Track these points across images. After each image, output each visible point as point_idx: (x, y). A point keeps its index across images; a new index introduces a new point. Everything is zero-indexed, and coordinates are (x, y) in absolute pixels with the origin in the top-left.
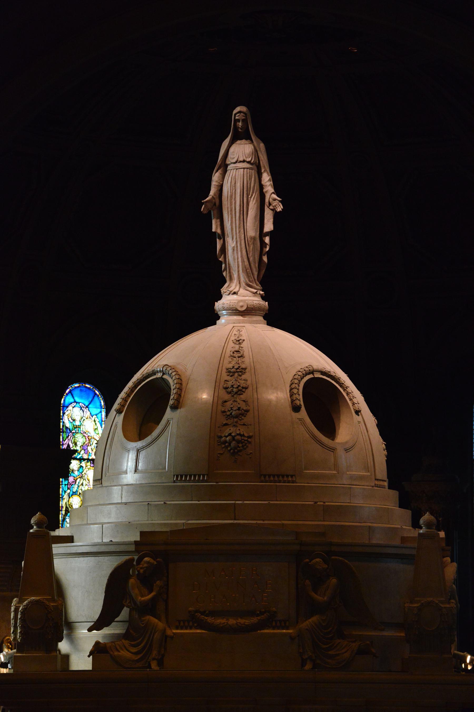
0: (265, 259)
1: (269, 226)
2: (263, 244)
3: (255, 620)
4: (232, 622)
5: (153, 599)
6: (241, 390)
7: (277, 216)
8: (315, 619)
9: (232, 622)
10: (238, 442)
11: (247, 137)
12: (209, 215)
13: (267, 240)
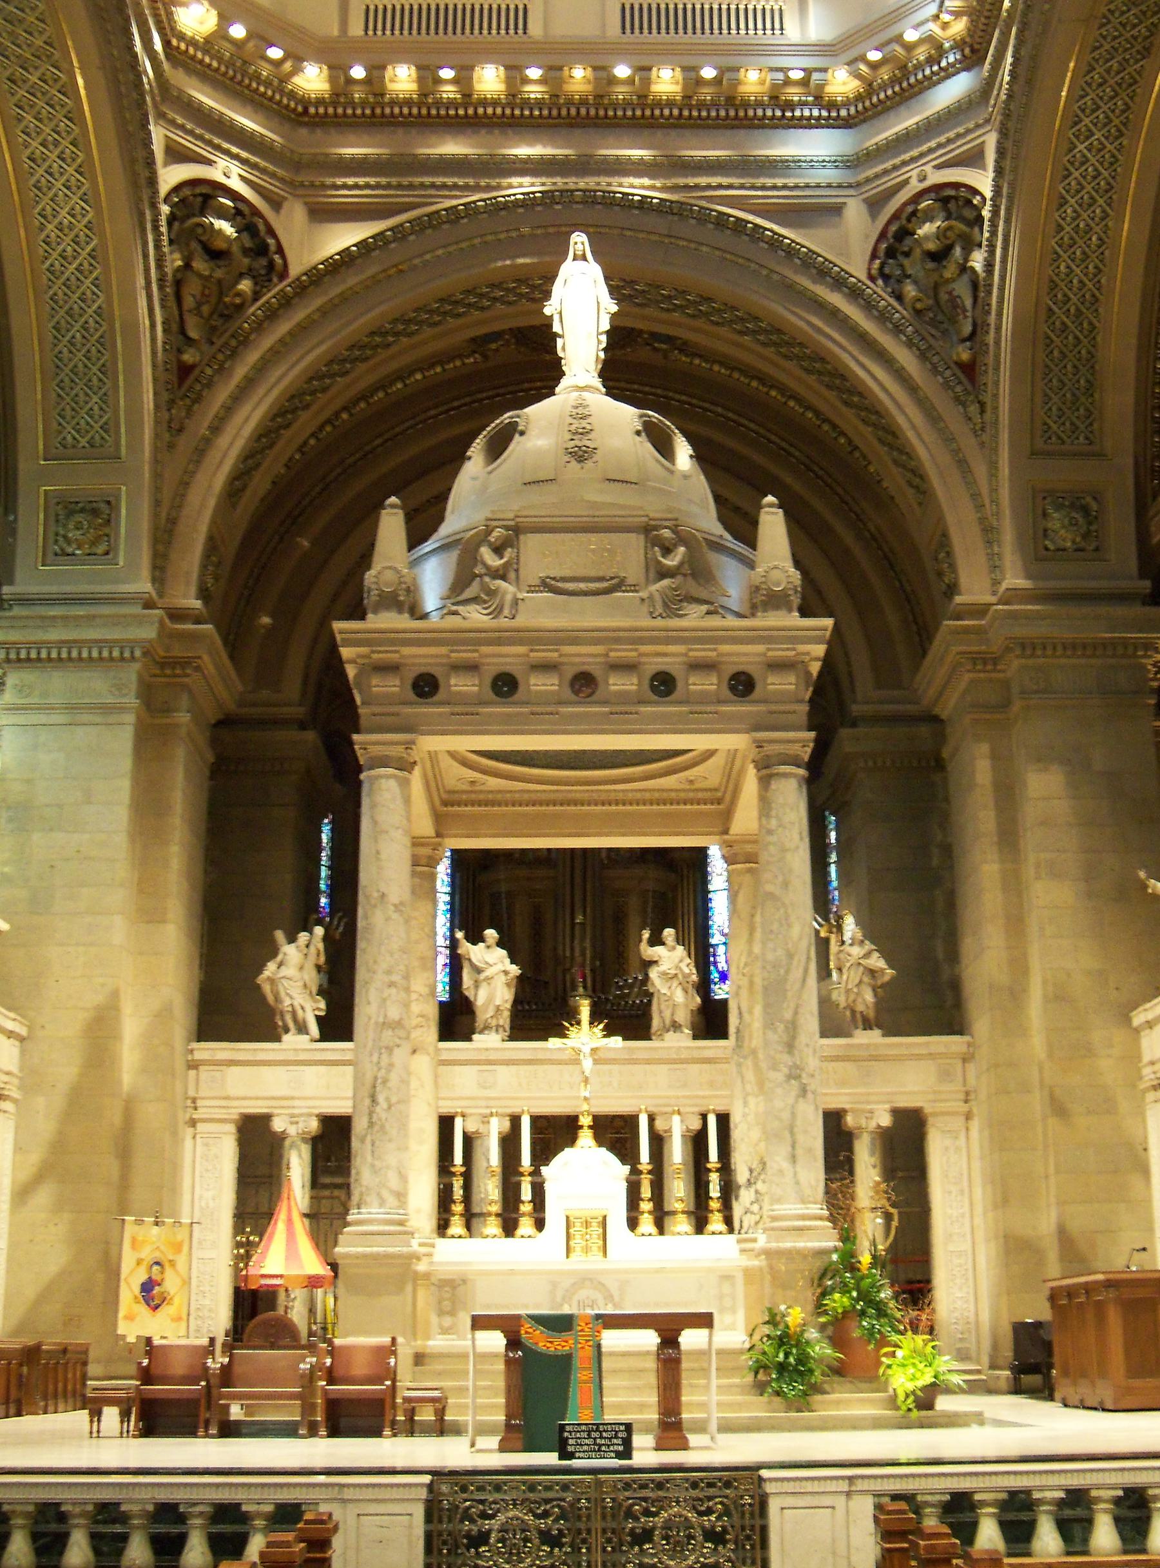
3: (605, 584)
4: (582, 586)
5: (506, 565)
8: (666, 582)
9: (582, 586)
10: (585, 452)
11: (584, 258)
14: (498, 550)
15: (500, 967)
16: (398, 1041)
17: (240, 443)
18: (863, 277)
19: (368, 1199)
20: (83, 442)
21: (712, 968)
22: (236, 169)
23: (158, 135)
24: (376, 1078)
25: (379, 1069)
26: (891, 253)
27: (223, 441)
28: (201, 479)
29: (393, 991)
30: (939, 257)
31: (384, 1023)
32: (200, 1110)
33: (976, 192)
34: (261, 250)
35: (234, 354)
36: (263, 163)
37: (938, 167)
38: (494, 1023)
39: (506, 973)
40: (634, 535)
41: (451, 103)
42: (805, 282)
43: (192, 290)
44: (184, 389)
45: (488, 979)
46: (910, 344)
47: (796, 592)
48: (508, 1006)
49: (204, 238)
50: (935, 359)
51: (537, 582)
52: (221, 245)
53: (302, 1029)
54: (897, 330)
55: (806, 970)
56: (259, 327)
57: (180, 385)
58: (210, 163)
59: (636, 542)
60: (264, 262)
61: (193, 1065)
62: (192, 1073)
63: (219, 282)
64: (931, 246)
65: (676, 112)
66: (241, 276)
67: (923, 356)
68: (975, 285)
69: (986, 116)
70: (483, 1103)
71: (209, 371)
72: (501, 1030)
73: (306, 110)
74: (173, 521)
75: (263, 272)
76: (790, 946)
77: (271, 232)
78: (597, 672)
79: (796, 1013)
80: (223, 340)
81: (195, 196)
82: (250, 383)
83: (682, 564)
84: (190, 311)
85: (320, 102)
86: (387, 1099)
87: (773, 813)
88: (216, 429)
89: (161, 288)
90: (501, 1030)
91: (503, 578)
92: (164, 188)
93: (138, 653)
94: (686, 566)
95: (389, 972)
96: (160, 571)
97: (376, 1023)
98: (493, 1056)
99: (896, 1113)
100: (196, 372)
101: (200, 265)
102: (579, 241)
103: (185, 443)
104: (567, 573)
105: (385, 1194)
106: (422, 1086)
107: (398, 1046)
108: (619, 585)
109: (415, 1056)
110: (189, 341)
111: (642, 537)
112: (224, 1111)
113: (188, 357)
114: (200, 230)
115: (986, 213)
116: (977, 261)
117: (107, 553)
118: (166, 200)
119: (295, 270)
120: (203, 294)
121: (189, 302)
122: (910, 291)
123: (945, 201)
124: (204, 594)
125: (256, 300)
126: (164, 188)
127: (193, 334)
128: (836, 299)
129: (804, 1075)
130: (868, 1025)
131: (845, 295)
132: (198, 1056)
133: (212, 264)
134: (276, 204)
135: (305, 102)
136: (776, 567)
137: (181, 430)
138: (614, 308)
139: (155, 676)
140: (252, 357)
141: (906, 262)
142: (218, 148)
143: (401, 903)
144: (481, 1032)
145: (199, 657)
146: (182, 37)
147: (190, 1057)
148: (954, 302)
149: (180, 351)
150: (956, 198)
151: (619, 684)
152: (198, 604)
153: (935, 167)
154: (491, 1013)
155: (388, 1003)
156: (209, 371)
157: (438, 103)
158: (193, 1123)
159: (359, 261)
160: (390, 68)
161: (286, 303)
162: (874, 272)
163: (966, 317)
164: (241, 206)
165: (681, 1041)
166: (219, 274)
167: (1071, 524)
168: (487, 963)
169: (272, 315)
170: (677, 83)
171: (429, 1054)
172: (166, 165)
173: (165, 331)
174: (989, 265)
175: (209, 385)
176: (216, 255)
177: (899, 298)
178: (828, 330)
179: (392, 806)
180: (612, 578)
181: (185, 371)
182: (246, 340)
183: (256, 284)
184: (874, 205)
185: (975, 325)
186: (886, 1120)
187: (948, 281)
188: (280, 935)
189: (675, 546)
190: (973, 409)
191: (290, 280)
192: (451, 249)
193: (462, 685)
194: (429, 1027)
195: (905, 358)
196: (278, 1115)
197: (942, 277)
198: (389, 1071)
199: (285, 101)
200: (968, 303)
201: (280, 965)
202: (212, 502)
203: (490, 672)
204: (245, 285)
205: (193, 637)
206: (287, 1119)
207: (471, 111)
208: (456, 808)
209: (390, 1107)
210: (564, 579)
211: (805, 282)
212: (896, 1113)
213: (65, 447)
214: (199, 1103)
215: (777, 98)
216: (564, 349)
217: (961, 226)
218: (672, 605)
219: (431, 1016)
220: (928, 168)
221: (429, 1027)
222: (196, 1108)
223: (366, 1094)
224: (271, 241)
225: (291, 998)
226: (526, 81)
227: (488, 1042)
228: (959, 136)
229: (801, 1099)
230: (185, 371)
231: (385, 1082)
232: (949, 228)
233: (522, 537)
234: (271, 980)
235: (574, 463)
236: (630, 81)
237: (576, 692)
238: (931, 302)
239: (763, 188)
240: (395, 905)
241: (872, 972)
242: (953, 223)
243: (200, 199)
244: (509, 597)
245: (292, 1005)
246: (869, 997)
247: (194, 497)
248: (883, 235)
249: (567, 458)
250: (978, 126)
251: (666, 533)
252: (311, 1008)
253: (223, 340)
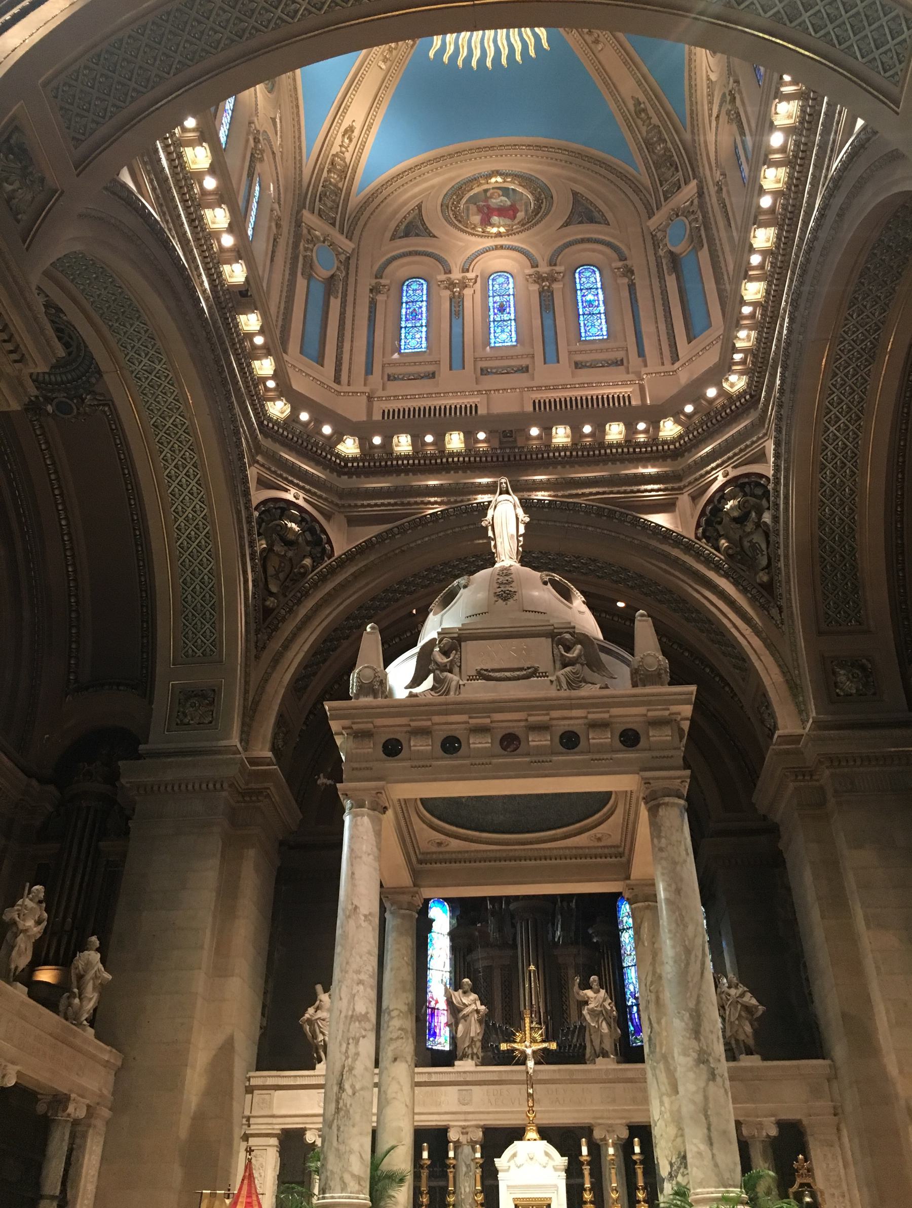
0: (520, 549)
1: (522, 530)
2: (518, 541)
4: (508, 674)
5: (451, 661)
6: (509, 583)
7: (527, 526)
8: (568, 669)
9: (508, 674)
11: (508, 493)
12: (486, 528)
13: (521, 539)
14: (445, 653)
15: (473, 1007)
16: (364, 1033)
17: (301, 655)
18: (693, 537)
19: (332, 1184)
20: (199, 653)
21: (630, 1023)
22: (301, 495)
23: (252, 473)
24: (344, 1067)
25: (347, 1058)
26: (708, 523)
27: (290, 654)
28: (276, 676)
29: (361, 987)
30: (740, 520)
31: (352, 1016)
32: (252, 1127)
33: (762, 476)
34: (318, 542)
35: (299, 602)
36: (319, 493)
37: (735, 467)
38: (470, 1051)
39: (477, 1011)
40: (543, 639)
41: (433, 457)
42: (654, 543)
43: (273, 562)
44: (266, 624)
45: (465, 1017)
46: (726, 576)
47: (666, 671)
48: (480, 1037)
49: (281, 533)
50: (745, 583)
51: (474, 673)
52: (291, 537)
54: (717, 568)
55: (703, 963)
56: (315, 586)
57: (264, 620)
58: (286, 490)
59: (546, 643)
60: (319, 549)
61: (250, 1090)
62: (249, 1096)
63: (291, 559)
64: (736, 514)
65: (568, 453)
66: (305, 557)
67: (736, 583)
68: (767, 535)
69: (764, 431)
70: (462, 1117)
71: (283, 612)
72: (475, 1057)
73: (346, 465)
74: (256, 703)
75: (319, 555)
76: (687, 943)
77: (324, 531)
78: (520, 732)
79: (698, 1002)
80: (292, 594)
81: (276, 509)
82: (308, 619)
83: (579, 656)
84: (272, 576)
85: (354, 459)
86: (353, 1087)
87: (663, 834)
88: (286, 646)
89: (252, 559)
90: (475, 1057)
91: (451, 671)
92: (255, 502)
93: (225, 785)
94: (583, 658)
95: (358, 972)
97: (346, 1017)
98: (469, 1078)
99: (781, 1124)
100: (275, 612)
101: (279, 548)
103: (267, 656)
104: (496, 666)
105: (347, 1177)
106: (402, 1090)
107: (364, 1037)
108: (534, 672)
109: (396, 1063)
110: (271, 594)
111: (550, 640)
112: (270, 1127)
113: (271, 602)
114: (279, 528)
115: (770, 487)
116: (767, 518)
117: (211, 722)
118: (256, 509)
120: (280, 566)
121: (271, 571)
122: (724, 543)
123: (742, 487)
124: (274, 749)
125: (313, 571)
126: (255, 502)
127: (274, 589)
128: (676, 552)
129: (711, 1060)
130: (750, 1052)
131: (682, 550)
132: (253, 1082)
133: (286, 548)
134: (328, 517)
135: (346, 460)
136: (649, 655)
137: (264, 648)
138: (527, 519)
139: (238, 802)
140: (310, 603)
141: (719, 527)
142: (292, 482)
143: (370, 914)
144: (461, 1059)
145: (268, 788)
146: (270, 419)
147: (247, 1084)
148: (753, 546)
149: (264, 600)
150: (749, 484)
151: (537, 740)
152: (270, 754)
153: (733, 467)
154: (467, 1044)
155: (356, 998)
156: (283, 612)
157: (425, 457)
158: (246, 1137)
159: (377, 546)
160: (395, 437)
161: (332, 571)
162: (699, 535)
163: (763, 555)
164: (304, 515)
165: (607, 1065)
166: (290, 554)
167: (854, 677)
168: (464, 1004)
169: (323, 579)
170: (568, 437)
171: (407, 1062)
172: (257, 489)
173: (254, 586)
174: (776, 519)
175: (284, 620)
176: (289, 543)
177: (718, 549)
178: (672, 571)
179: (365, 837)
180: (529, 668)
181: (267, 612)
182: (306, 594)
183: (314, 562)
184: (695, 498)
185: (769, 559)
186: (774, 1132)
187: (749, 534)
188: (319, 988)
189: (575, 644)
190: (774, 612)
191: (333, 558)
192: (433, 537)
194: (408, 1039)
196: (310, 1129)
197: (744, 531)
198: (354, 1060)
199: (334, 459)
200: (764, 546)
201: (317, 1009)
202: (282, 691)
203: (440, 736)
204: (307, 562)
206: (316, 1132)
207: (444, 460)
208: (429, 865)
209: (354, 1094)
210: (493, 670)
211: (654, 543)
212: (781, 1124)
213: (187, 656)
214: (252, 1121)
215: (630, 441)
216: (495, 546)
217: (752, 500)
218: (574, 683)
219: (409, 1030)
220: (729, 469)
221: (408, 1039)
222: (249, 1126)
223: (335, 1082)
224: (324, 537)
225: (323, 1034)
226: (478, 441)
228: (747, 447)
229: (711, 1083)
231: (351, 1069)
232: (747, 501)
233: (463, 644)
234: (310, 1022)
235: (500, 601)
236: (539, 437)
237: (504, 749)
238: (738, 549)
239: (625, 492)
240: (365, 916)
241: (747, 1008)
242: (749, 498)
243: (279, 511)
244: (454, 683)
245: (324, 1040)
246: (748, 1029)
247: (270, 689)
248: (703, 513)
249: (496, 599)
250: (759, 439)
251: (568, 636)
253: (292, 594)
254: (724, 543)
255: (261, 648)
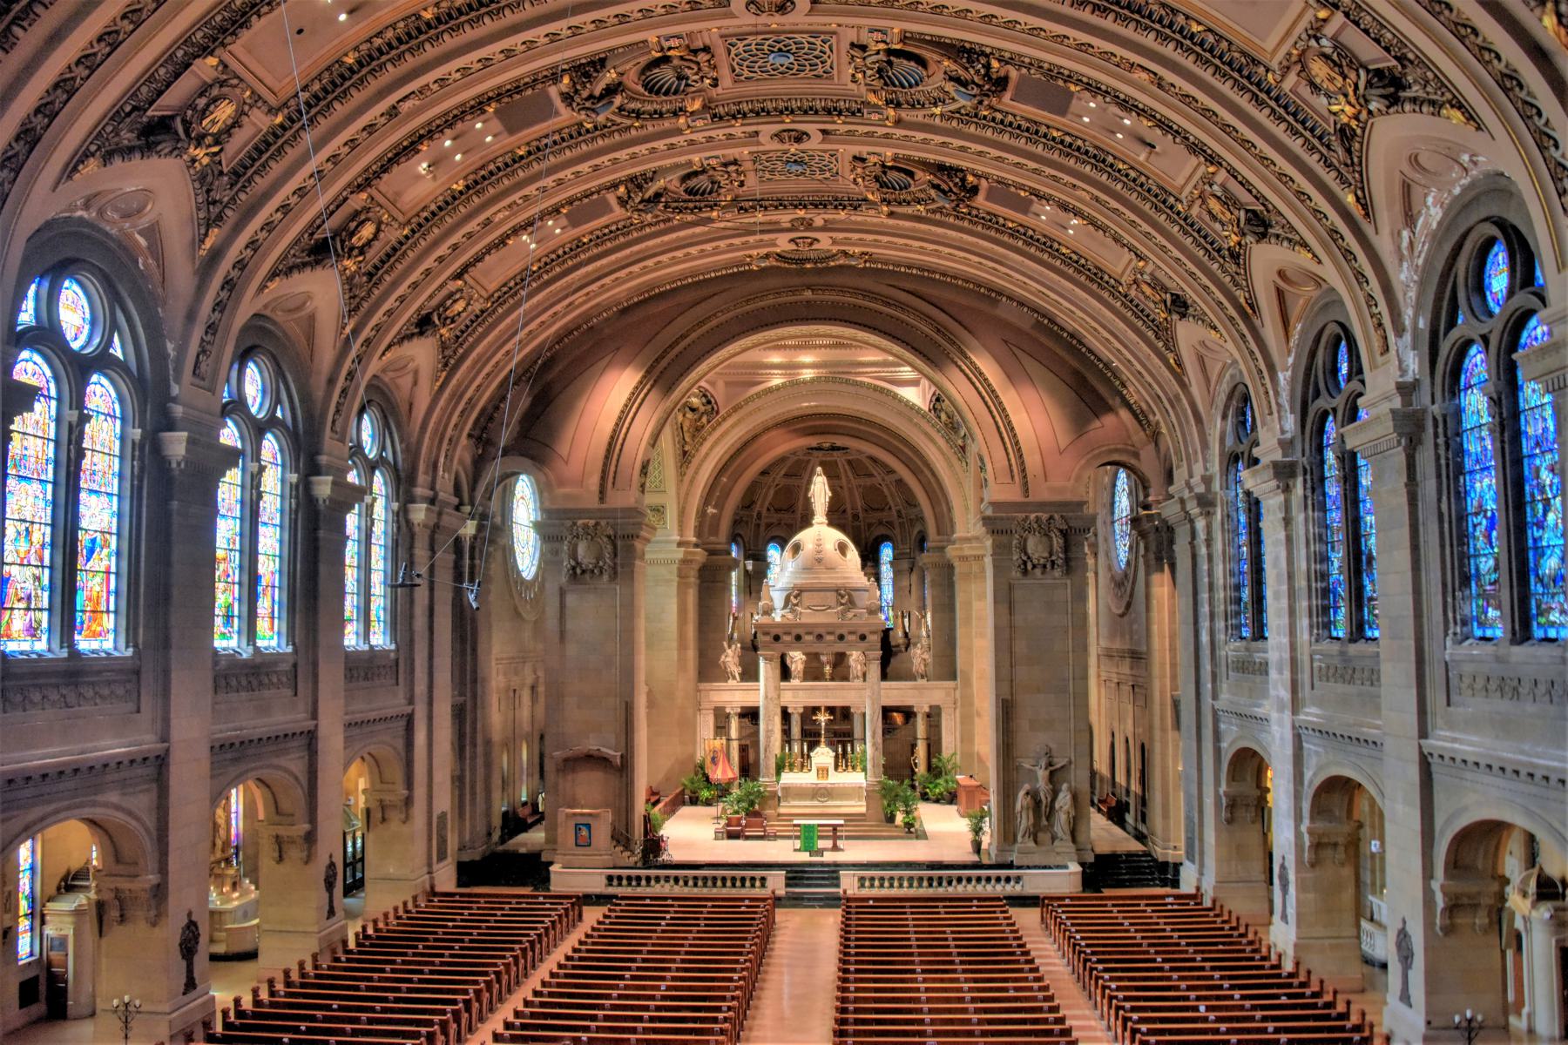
14: (796, 597)
34: (709, 402)
53: (734, 678)
56: (710, 434)
59: (834, 594)
74: (684, 508)
96: (681, 531)
99: (931, 707)
101: (690, 415)
102: (819, 469)
103: (687, 479)
108: (830, 608)
119: (723, 412)
121: (685, 429)
122: (943, 416)
127: (687, 439)
130: (922, 677)
140: (707, 445)
161: (719, 424)
165: (858, 683)
169: (714, 429)
176: (693, 410)
181: (685, 453)
182: (705, 439)
193: (787, 638)
195: (942, 443)
204: (704, 419)
205: (694, 553)
212: (931, 707)
227: (795, 682)
230: (685, 453)
252: (736, 670)
254: (943, 416)
255: (683, 475)
